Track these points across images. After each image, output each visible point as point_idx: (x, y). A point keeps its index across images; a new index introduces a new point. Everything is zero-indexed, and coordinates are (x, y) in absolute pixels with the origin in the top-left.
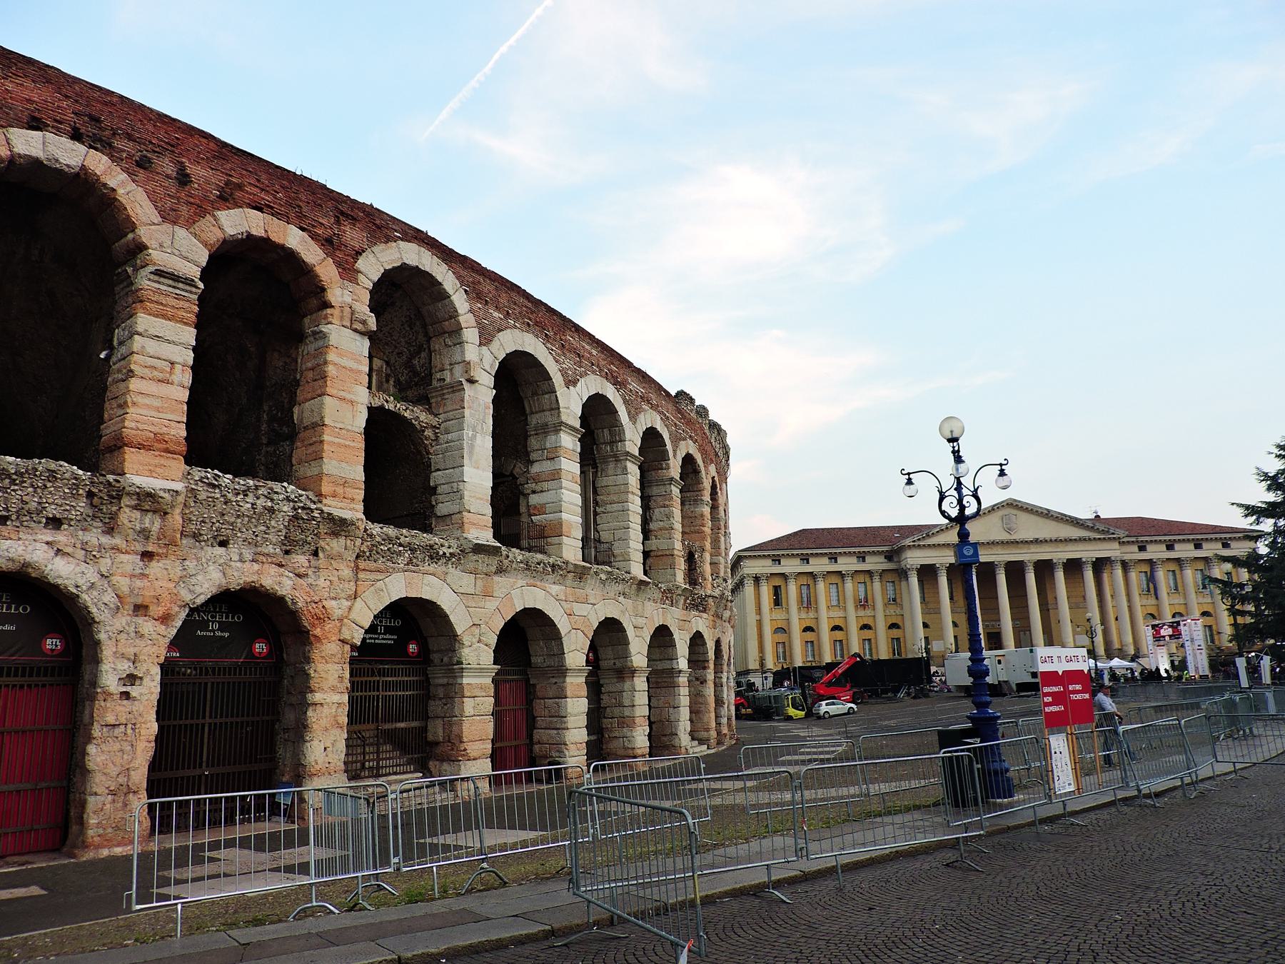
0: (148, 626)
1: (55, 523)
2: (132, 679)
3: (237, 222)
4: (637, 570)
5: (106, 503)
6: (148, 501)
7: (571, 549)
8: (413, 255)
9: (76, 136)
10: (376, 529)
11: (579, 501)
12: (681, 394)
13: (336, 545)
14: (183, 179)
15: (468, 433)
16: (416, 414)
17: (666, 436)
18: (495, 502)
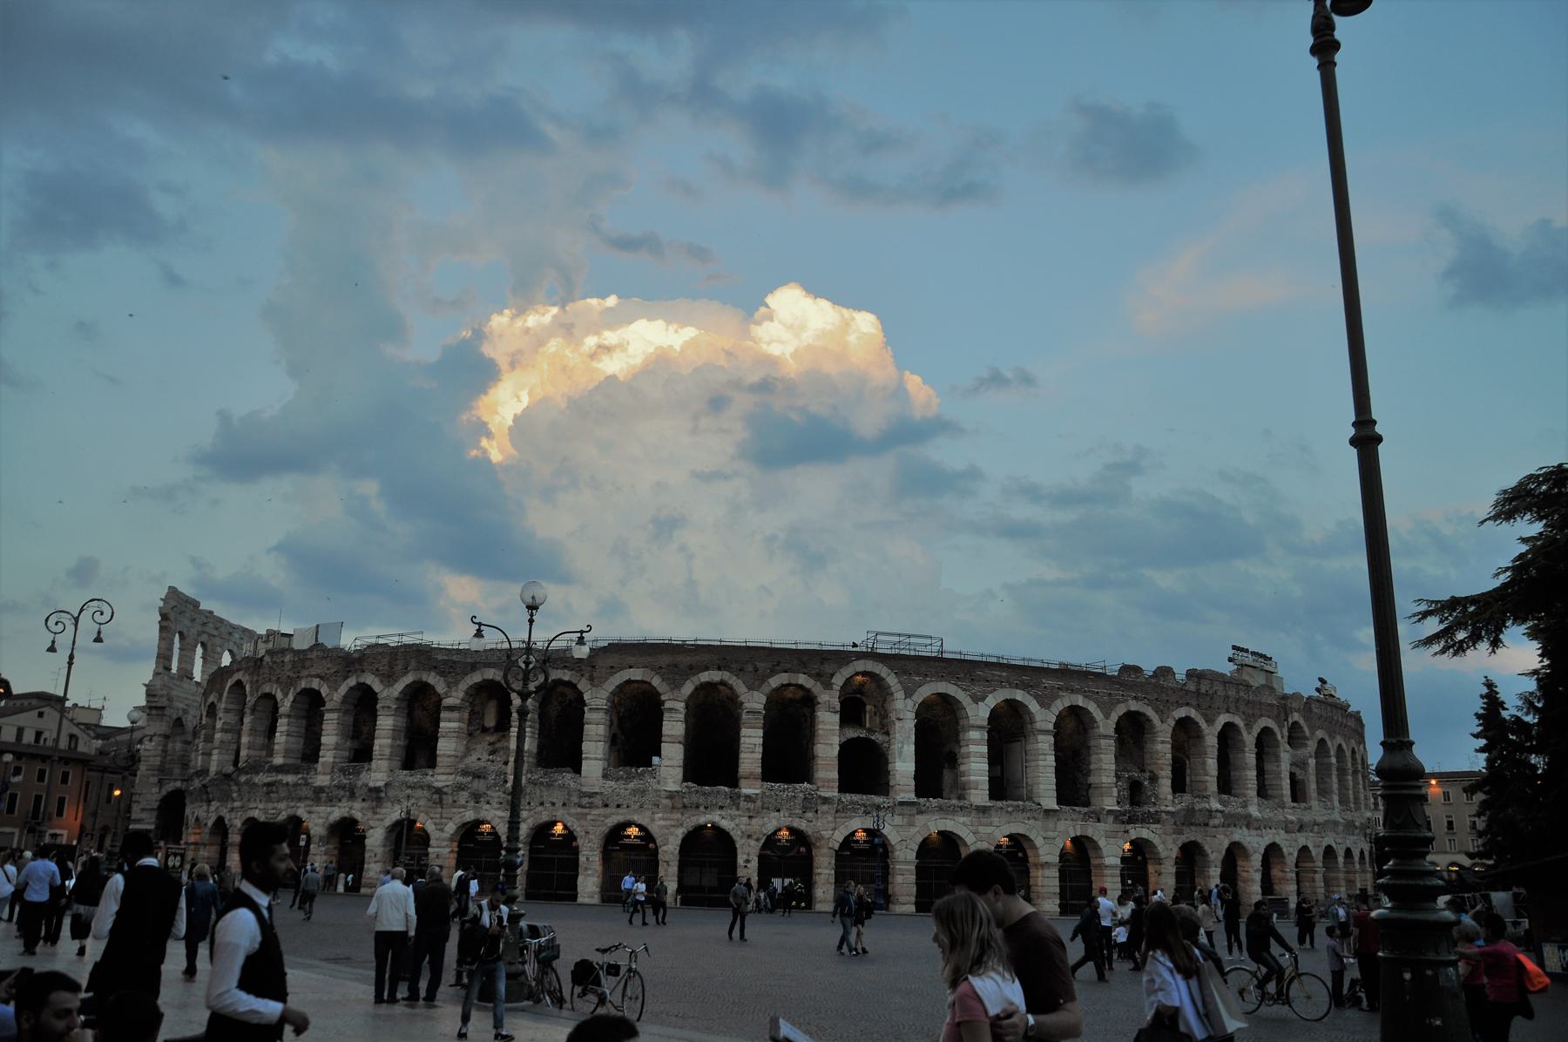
0: (753, 843)
1: (721, 808)
2: (748, 861)
3: (775, 682)
4: (1050, 802)
5: (735, 799)
6: (748, 798)
7: (979, 795)
8: (860, 666)
9: (719, 669)
10: (847, 797)
11: (986, 767)
12: (1126, 669)
13: (825, 807)
14: (756, 670)
15: (895, 747)
16: (878, 737)
17: (1092, 707)
18: (916, 778)
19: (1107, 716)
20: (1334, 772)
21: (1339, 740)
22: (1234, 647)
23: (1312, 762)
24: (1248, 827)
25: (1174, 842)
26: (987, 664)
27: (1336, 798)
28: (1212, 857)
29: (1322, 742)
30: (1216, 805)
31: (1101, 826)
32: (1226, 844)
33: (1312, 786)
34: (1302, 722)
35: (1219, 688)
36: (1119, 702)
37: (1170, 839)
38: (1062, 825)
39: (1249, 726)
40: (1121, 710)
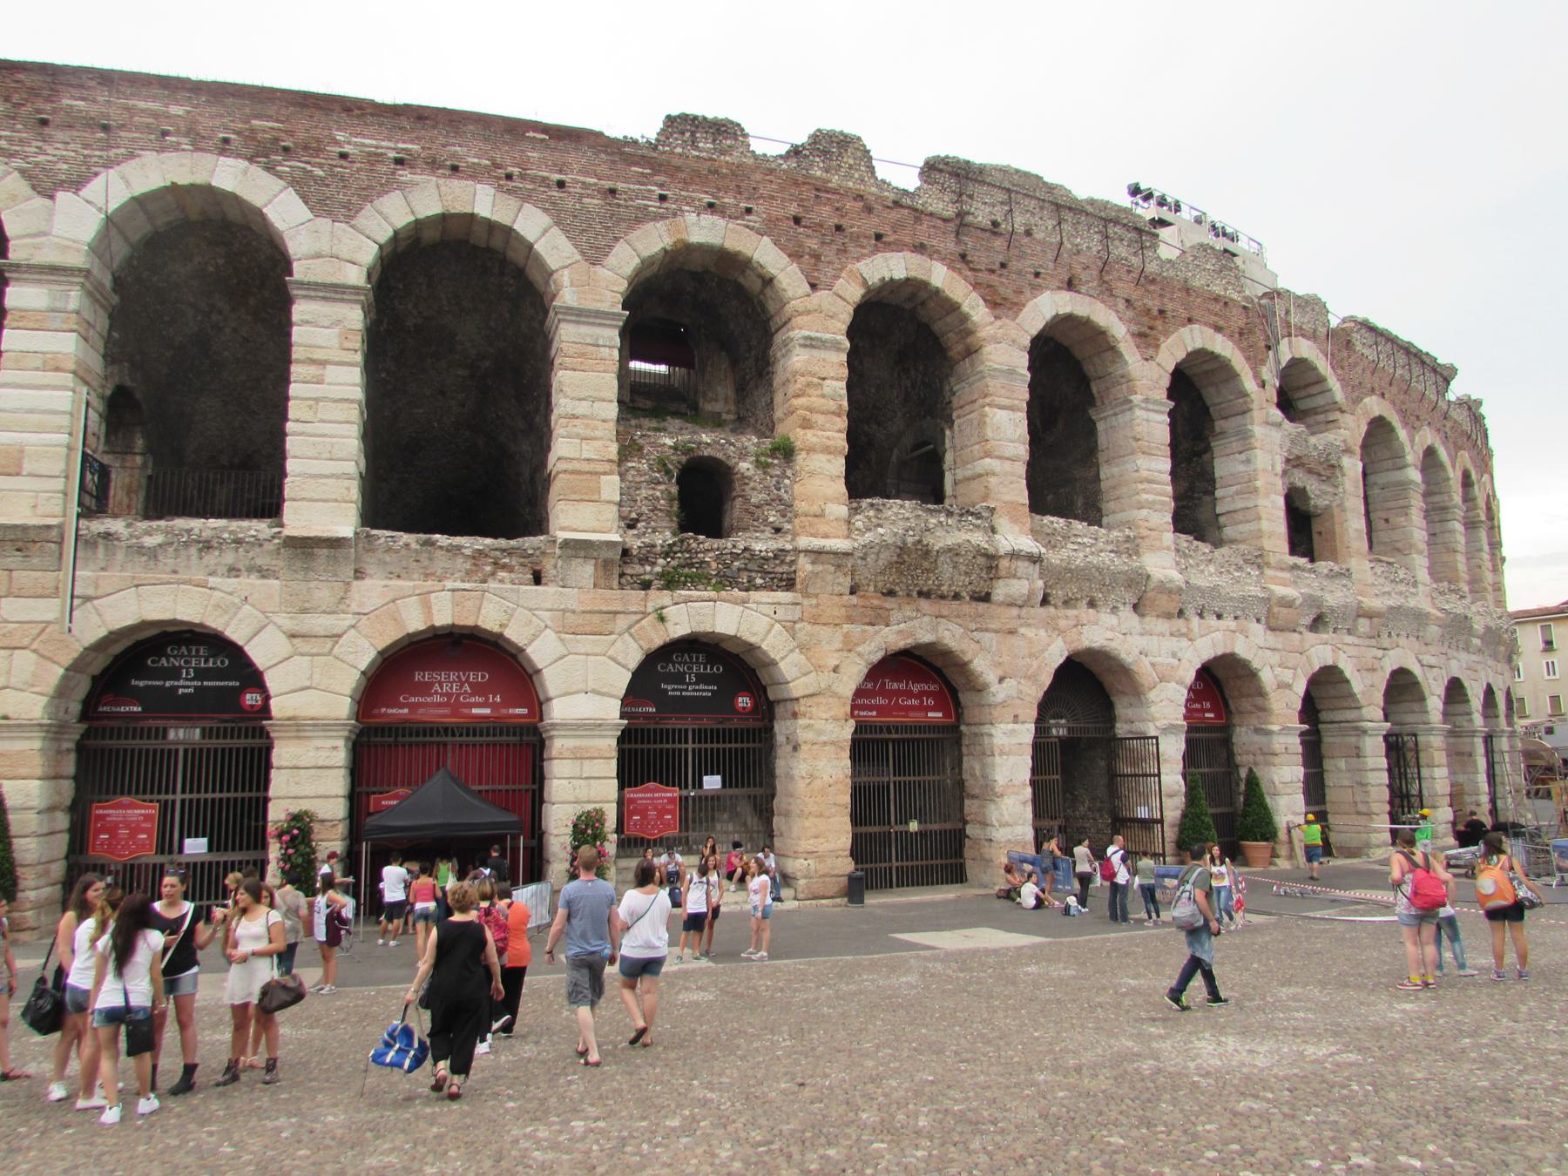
12: (680, 125)
17: (531, 224)
19: (595, 255)
20: (1417, 503)
21: (1427, 437)
22: (1135, 191)
23: (1352, 466)
24: (1135, 607)
25: (849, 646)
26: (106, 78)
27: (1420, 563)
28: (999, 692)
29: (1379, 427)
30: (1014, 536)
31: (547, 593)
32: (1056, 655)
33: (1355, 523)
34: (1323, 366)
35: (1044, 228)
36: (642, 217)
37: (829, 642)
38: (372, 591)
39: (1147, 339)
40: (652, 240)
